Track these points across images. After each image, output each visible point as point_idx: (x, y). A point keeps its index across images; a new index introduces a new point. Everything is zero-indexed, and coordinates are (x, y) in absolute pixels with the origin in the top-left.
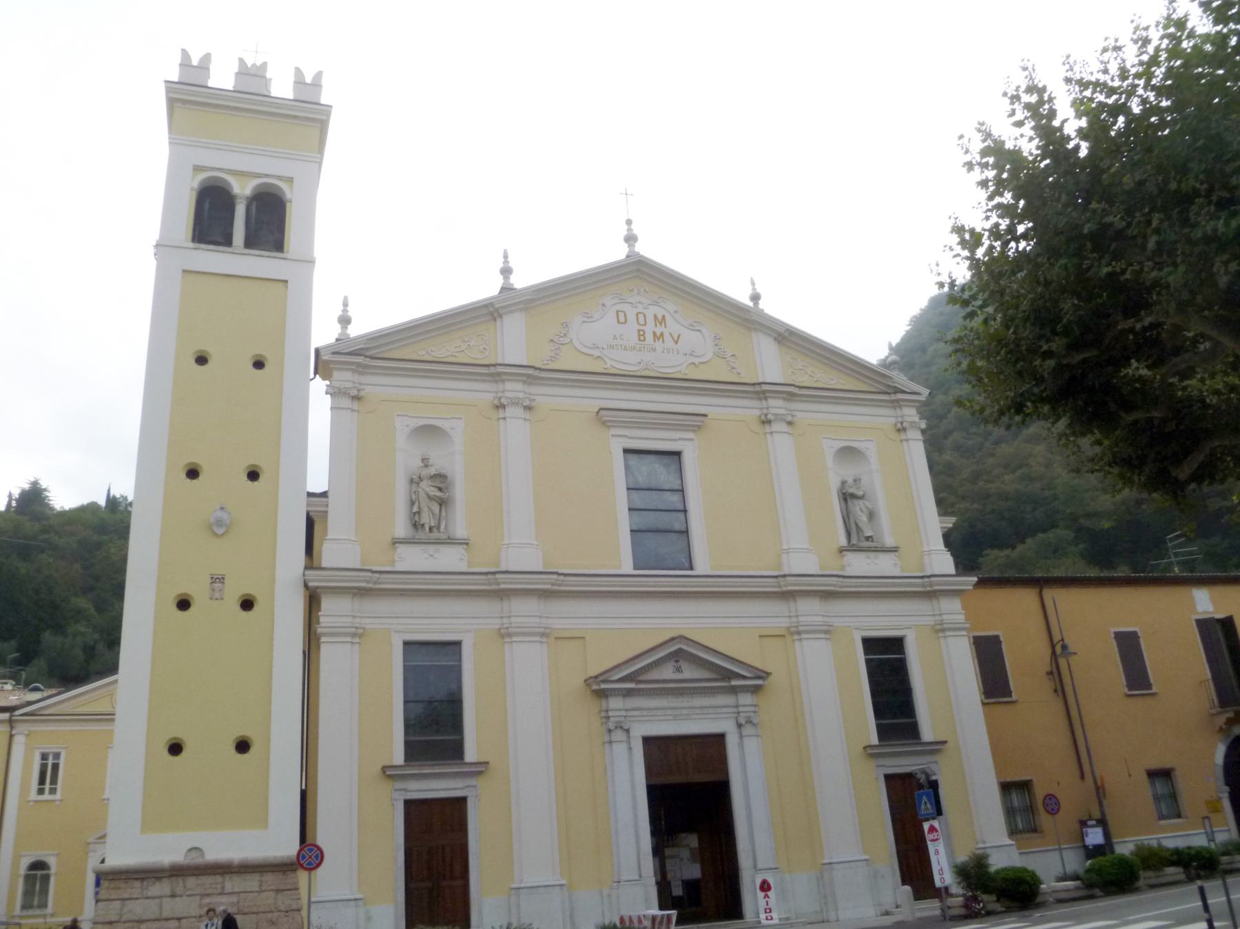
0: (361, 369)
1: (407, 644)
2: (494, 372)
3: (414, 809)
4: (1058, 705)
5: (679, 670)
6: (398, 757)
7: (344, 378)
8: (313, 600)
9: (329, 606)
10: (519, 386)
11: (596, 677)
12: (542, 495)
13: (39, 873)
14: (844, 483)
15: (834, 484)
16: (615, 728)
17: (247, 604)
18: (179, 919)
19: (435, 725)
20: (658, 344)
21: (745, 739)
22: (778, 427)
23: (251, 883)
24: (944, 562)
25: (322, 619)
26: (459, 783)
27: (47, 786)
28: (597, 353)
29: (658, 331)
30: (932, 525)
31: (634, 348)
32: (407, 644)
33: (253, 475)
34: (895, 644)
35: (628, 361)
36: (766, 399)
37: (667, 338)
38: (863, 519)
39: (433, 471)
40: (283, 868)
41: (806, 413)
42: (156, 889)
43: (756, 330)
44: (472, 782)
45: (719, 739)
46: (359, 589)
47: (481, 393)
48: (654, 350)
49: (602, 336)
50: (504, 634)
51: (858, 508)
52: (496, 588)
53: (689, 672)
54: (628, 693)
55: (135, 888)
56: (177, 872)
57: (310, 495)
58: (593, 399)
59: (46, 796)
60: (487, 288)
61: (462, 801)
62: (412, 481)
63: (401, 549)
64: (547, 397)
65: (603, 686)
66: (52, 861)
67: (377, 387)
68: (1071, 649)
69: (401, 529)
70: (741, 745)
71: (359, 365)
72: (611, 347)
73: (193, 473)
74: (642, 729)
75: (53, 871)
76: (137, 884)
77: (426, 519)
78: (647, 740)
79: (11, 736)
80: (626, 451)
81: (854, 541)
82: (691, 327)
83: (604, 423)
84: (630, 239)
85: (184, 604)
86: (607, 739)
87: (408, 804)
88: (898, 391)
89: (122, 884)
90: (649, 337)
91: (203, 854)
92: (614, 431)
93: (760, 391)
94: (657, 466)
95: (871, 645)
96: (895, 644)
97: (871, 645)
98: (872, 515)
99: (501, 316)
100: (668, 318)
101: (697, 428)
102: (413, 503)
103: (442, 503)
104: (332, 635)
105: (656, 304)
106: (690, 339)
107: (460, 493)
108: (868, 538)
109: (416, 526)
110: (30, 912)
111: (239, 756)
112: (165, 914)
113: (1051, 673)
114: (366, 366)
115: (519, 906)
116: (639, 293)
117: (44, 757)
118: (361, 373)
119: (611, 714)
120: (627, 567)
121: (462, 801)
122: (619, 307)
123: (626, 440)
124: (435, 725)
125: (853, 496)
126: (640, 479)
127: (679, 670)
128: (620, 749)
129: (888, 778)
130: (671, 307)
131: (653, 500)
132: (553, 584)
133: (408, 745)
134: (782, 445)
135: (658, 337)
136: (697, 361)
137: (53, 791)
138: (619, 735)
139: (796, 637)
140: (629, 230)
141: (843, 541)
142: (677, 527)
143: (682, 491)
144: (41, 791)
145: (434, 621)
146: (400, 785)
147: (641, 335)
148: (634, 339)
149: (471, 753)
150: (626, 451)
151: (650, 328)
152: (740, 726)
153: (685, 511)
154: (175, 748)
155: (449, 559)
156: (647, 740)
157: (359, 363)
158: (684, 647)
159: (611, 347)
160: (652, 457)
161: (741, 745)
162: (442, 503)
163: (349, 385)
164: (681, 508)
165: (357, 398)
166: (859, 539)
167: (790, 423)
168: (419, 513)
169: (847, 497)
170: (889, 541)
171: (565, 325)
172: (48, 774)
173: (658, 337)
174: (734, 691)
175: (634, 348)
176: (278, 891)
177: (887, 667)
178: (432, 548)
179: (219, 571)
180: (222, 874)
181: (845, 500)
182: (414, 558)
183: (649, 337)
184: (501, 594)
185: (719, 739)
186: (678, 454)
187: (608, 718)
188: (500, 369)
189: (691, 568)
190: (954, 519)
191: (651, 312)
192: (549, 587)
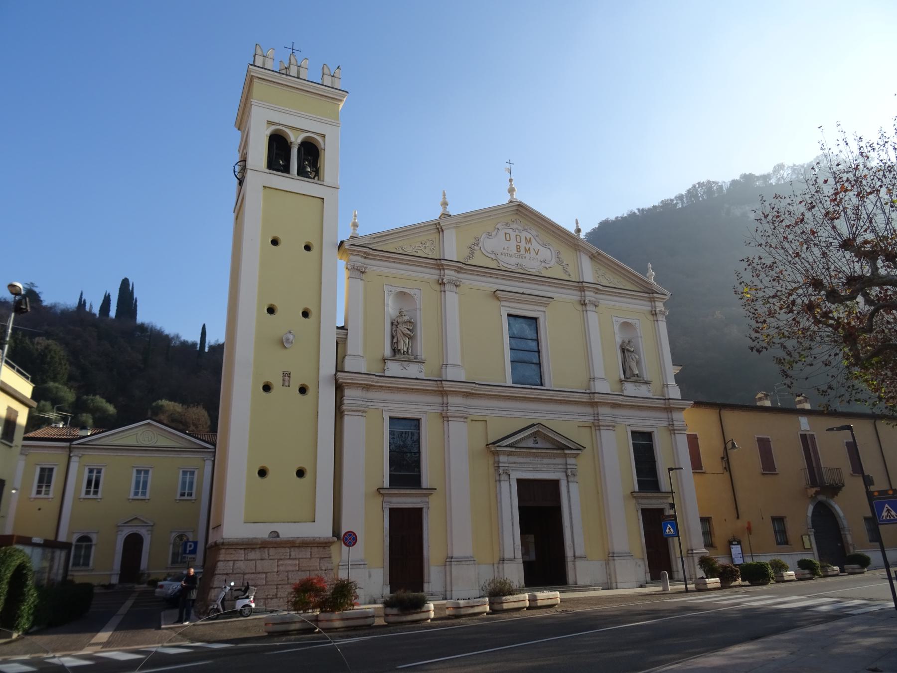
0: (367, 256)
1: (391, 418)
2: (439, 264)
3: (395, 514)
4: (727, 474)
6: (387, 484)
7: (359, 260)
8: (339, 388)
9: (348, 392)
10: (453, 273)
11: (494, 443)
12: (467, 337)
13: (84, 544)
14: (623, 342)
15: (619, 340)
16: (499, 473)
17: (303, 390)
18: (266, 573)
19: (405, 465)
20: (527, 255)
21: (571, 484)
23: (306, 553)
24: (675, 392)
25: (345, 401)
26: (418, 500)
27: (92, 490)
28: (493, 256)
30: (671, 371)
31: (514, 256)
32: (391, 418)
33: (305, 314)
34: (649, 436)
35: (509, 262)
37: (532, 251)
38: (633, 365)
39: (406, 318)
40: (324, 545)
41: (605, 302)
42: (253, 555)
43: (580, 251)
44: (426, 499)
45: (556, 483)
46: (367, 385)
49: (502, 247)
50: (445, 417)
52: (440, 388)
54: (510, 454)
55: (241, 554)
56: (263, 545)
57: (338, 328)
58: (491, 284)
59: (91, 496)
60: (433, 214)
61: (421, 510)
62: (392, 324)
63: (389, 364)
64: (469, 282)
65: (498, 449)
66: (94, 537)
67: (375, 267)
69: (388, 352)
70: (568, 487)
71: (365, 253)
72: (502, 254)
73: (271, 310)
74: (516, 475)
75: (94, 542)
76: (242, 551)
77: (402, 347)
78: (520, 482)
79: (70, 457)
80: (509, 315)
81: (628, 375)
82: (544, 246)
83: (498, 298)
84: (511, 191)
85: (267, 388)
86: (498, 478)
87: (392, 511)
88: (654, 292)
89: (232, 551)
90: (522, 249)
91: (278, 536)
92: (503, 303)
93: (581, 287)
96: (649, 436)
98: (638, 363)
100: (533, 240)
102: (393, 337)
103: (411, 338)
104: (349, 411)
105: (526, 230)
106: (545, 253)
107: (420, 332)
108: (634, 375)
109: (395, 351)
110: (77, 568)
111: (298, 479)
112: (259, 569)
113: (723, 458)
114: (369, 254)
115: (451, 572)
117: (91, 471)
118: (365, 258)
120: (509, 382)
121: (420, 510)
122: (508, 231)
124: (405, 465)
125: (628, 350)
127: (536, 442)
128: (505, 486)
129: (643, 510)
130: (534, 233)
131: (522, 345)
133: (392, 478)
134: (593, 317)
135: (527, 250)
137: (96, 493)
138: (504, 477)
140: (511, 185)
141: (622, 377)
142: (534, 361)
143: (537, 340)
144: (88, 493)
146: (386, 499)
147: (518, 248)
148: (513, 250)
149: (426, 482)
150: (509, 315)
151: (523, 244)
152: (567, 476)
153: (539, 352)
154: (262, 473)
155: (413, 370)
156: (520, 482)
157: (364, 252)
159: (502, 254)
160: (521, 320)
161: (568, 487)
162: (411, 338)
163: (359, 264)
164: (536, 349)
165: (363, 272)
166: (629, 375)
167: (596, 306)
170: (647, 376)
171: (478, 239)
172: (93, 484)
173: (527, 250)
175: (514, 256)
176: (321, 558)
177: (644, 448)
178: (405, 364)
179: (287, 370)
180: (290, 548)
181: (624, 352)
182: (394, 368)
183: (522, 249)
185: (556, 483)
186: (535, 319)
187: (499, 467)
188: (443, 262)
189: (542, 385)
190: (680, 368)
191: (524, 235)
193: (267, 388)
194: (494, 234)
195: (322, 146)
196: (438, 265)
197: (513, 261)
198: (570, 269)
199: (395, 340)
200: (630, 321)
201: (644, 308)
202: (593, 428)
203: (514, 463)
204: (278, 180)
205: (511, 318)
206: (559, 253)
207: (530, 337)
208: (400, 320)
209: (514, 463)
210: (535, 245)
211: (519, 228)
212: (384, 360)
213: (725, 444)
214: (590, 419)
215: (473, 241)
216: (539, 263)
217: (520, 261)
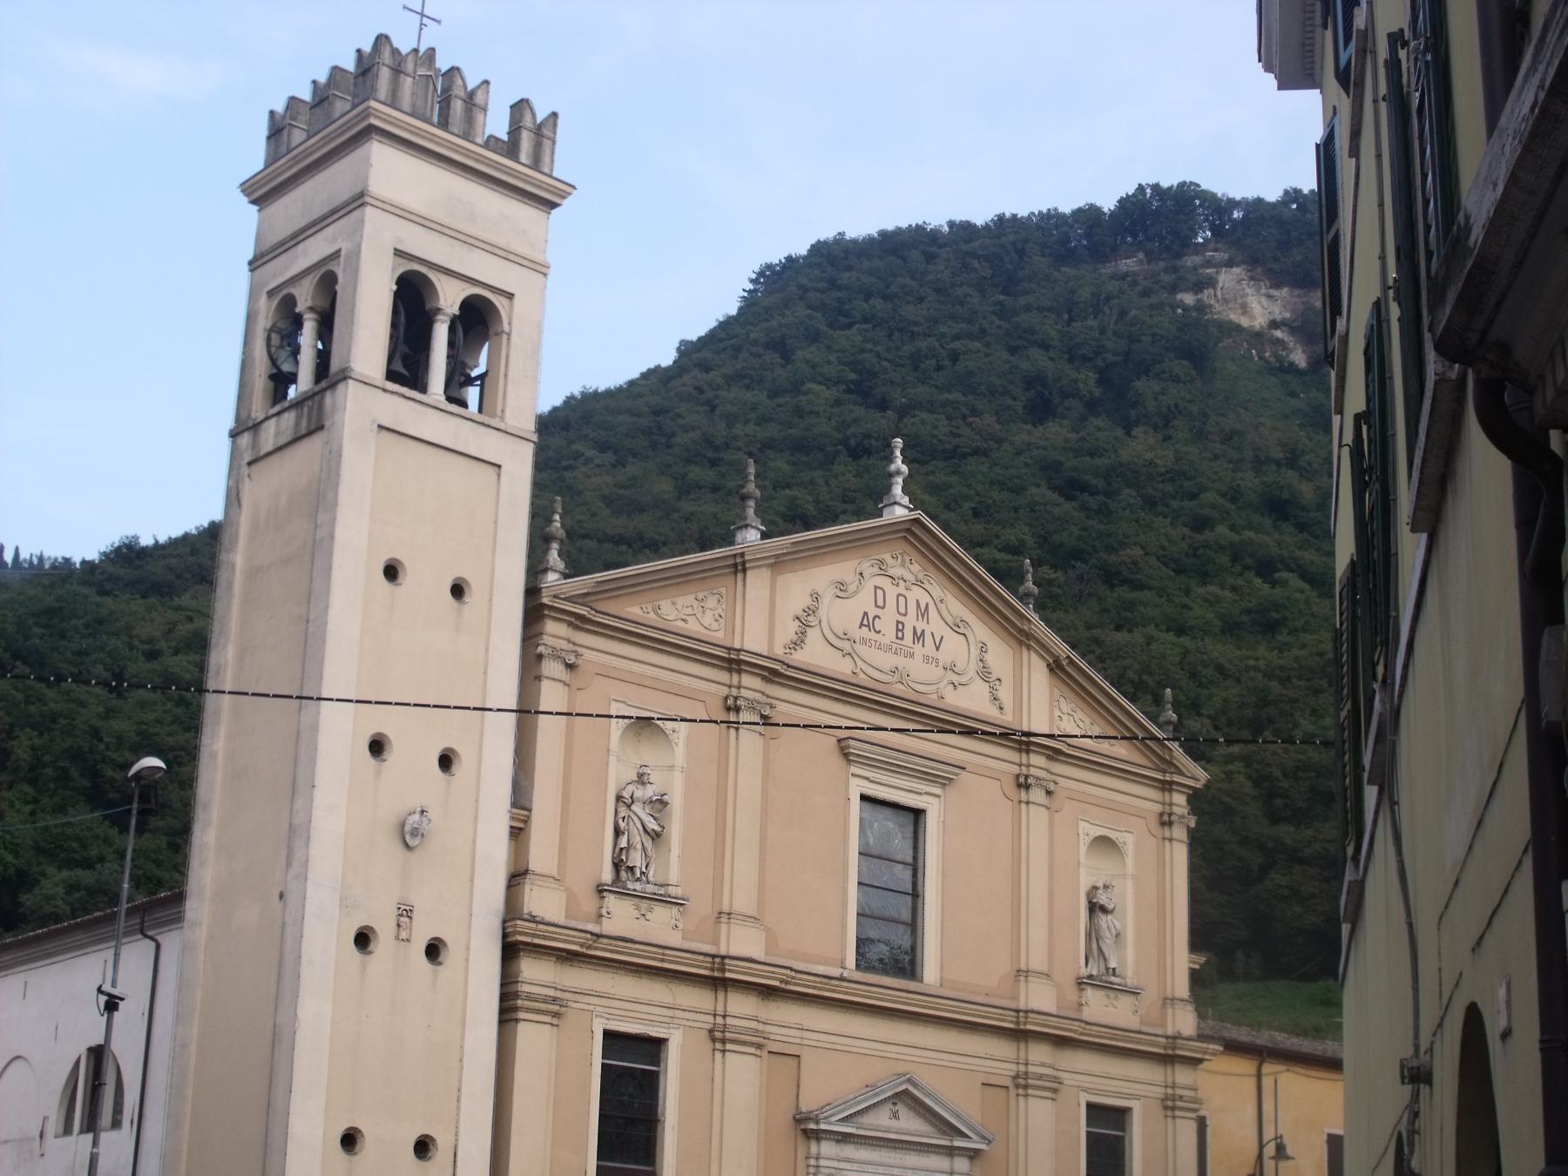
1: (609, 1035)
5: (895, 1116)
8: (510, 951)
17: (434, 950)
20: (918, 647)
22: (1037, 795)
28: (846, 646)
29: (920, 626)
32: (609, 1035)
36: (1028, 752)
41: (1070, 778)
43: (1029, 647)
47: (710, 684)
48: (912, 656)
51: (1104, 920)
53: (909, 1124)
54: (844, 1138)
62: (619, 798)
63: (611, 900)
68: (1289, 1151)
83: (846, 755)
85: (363, 939)
92: (854, 769)
93: (1023, 741)
94: (891, 825)
95: (1096, 1112)
97: (1096, 1112)
99: (744, 571)
101: (945, 782)
102: (618, 832)
104: (529, 1010)
105: (919, 583)
106: (955, 648)
116: (903, 565)
118: (577, 628)
119: (822, 1162)
123: (865, 783)
125: (1104, 910)
126: (871, 841)
127: (895, 1116)
132: (782, 981)
135: (919, 637)
136: (955, 678)
139: (1021, 1091)
145: (639, 1006)
147: (900, 627)
151: (910, 621)
154: (350, 1140)
158: (911, 1088)
160: (887, 812)
168: (628, 849)
169: (1095, 908)
171: (816, 597)
173: (919, 637)
174: (951, 1152)
184: (718, 983)
186: (917, 814)
192: (776, 983)
193: (363, 939)
194: (852, 588)
195: (506, 327)
196: (730, 661)
197: (886, 661)
198: (1005, 694)
199: (623, 843)
200: (1112, 835)
201: (1149, 805)
202: (1013, 1091)
203: (846, 1160)
204: (398, 408)
205: (867, 805)
206: (983, 648)
207: (899, 858)
208: (639, 793)
209: (846, 1160)
210: (935, 626)
211: (908, 576)
212: (601, 890)
213: (1261, 1146)
214: (1011, 1069)
215: (808, 601)
216: (940, 671)
217: (900, 661)
